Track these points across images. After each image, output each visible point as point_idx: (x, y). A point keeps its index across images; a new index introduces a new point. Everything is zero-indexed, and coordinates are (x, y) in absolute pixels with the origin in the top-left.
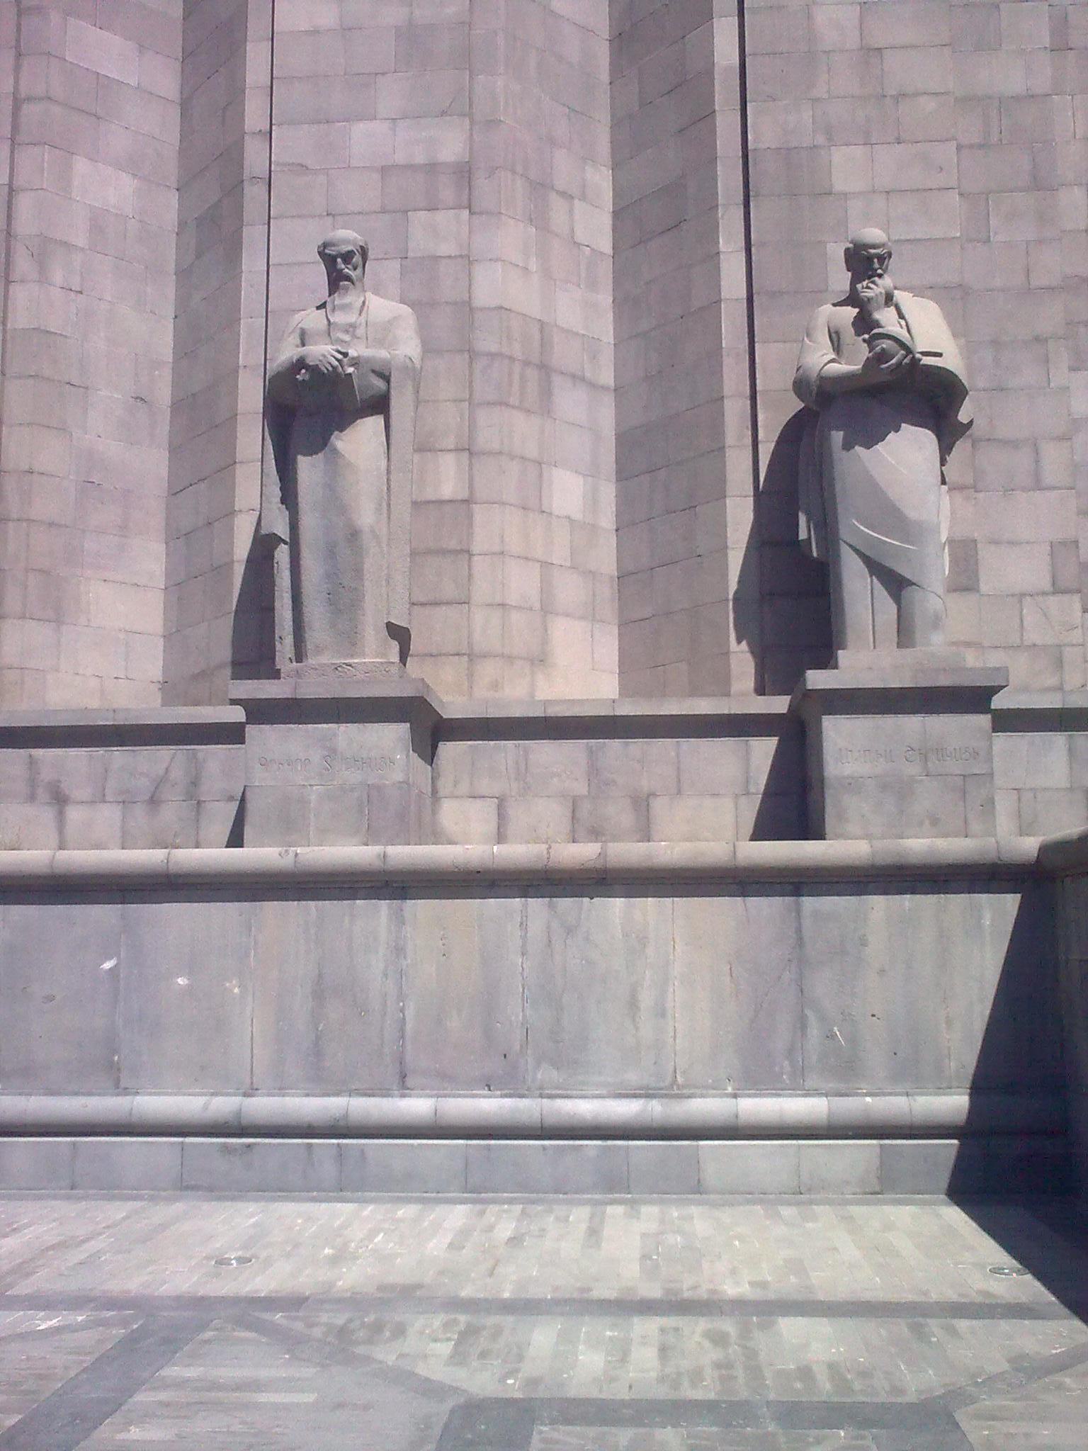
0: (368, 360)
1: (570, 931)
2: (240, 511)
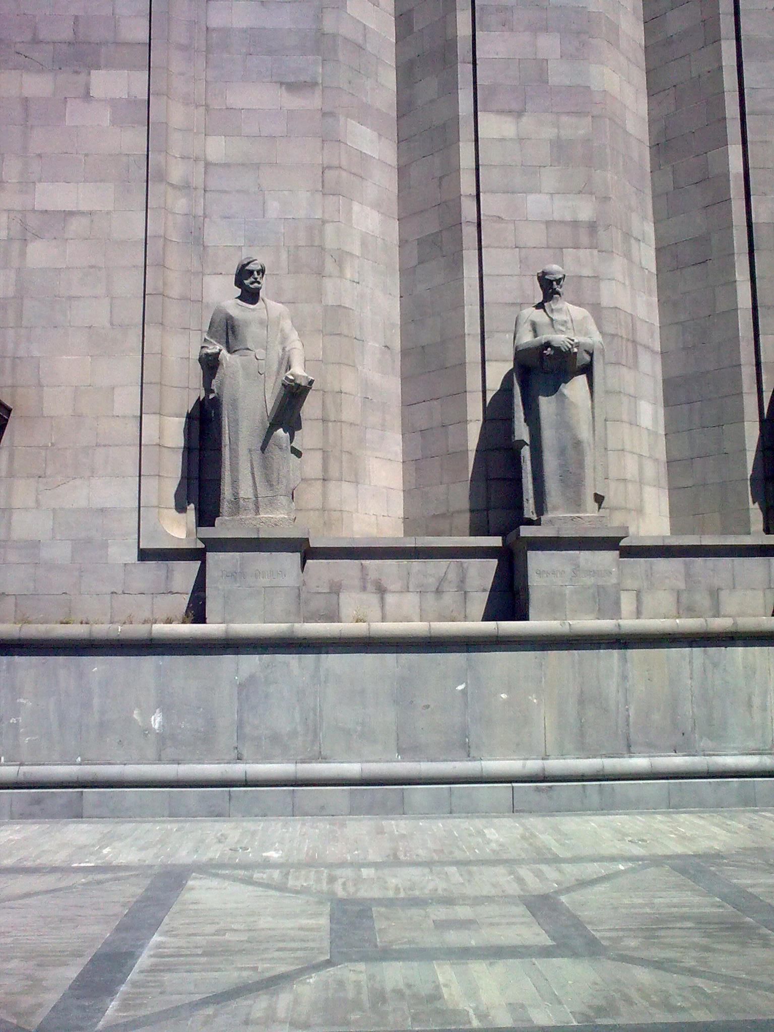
0: (584, 344)
1: (715, 665)
2: (471, 421)
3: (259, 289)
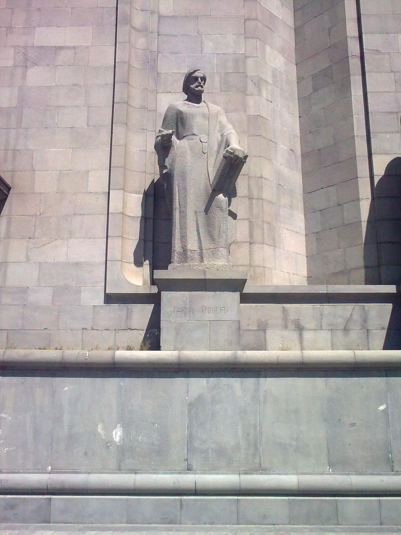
3: (202, 92)
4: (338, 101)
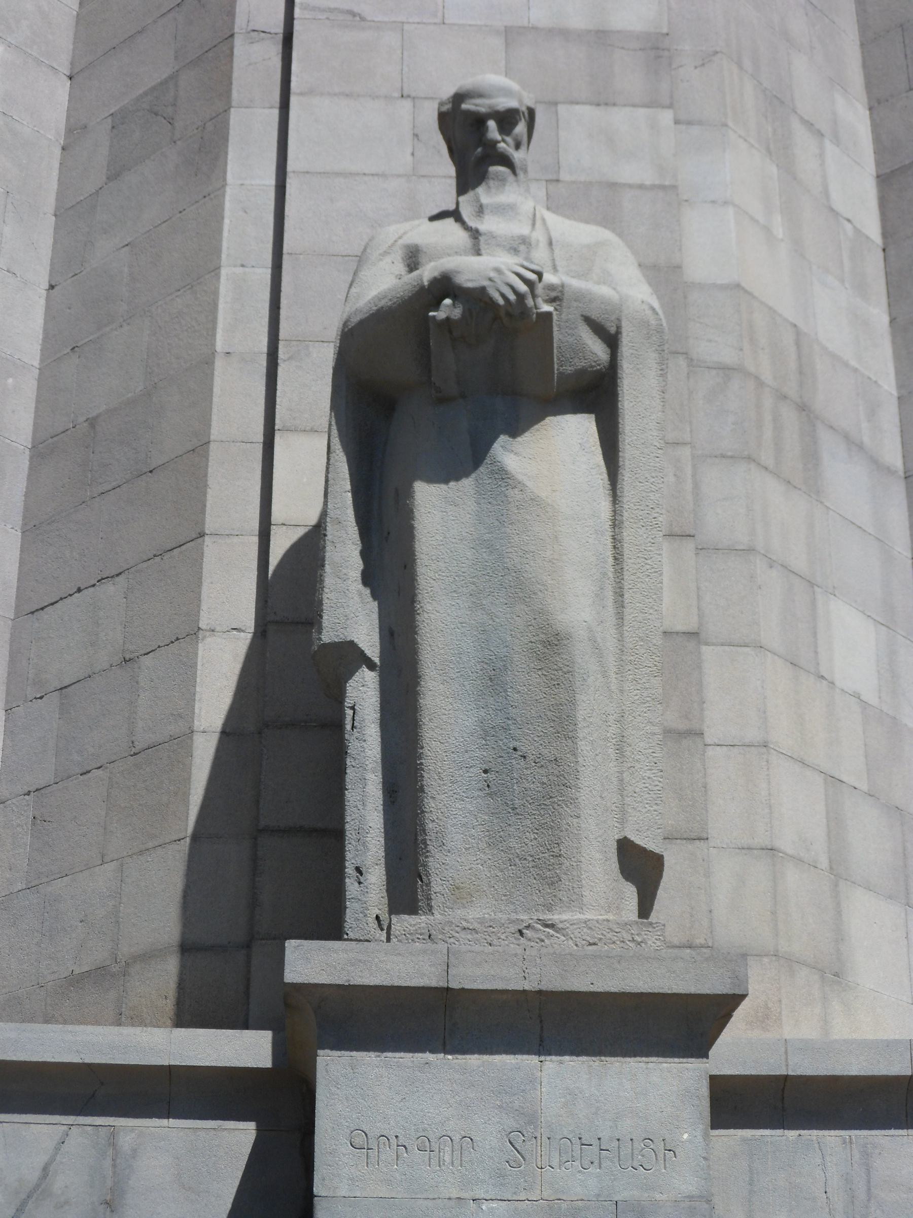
0: (579, 296)
4: (180, 212)
